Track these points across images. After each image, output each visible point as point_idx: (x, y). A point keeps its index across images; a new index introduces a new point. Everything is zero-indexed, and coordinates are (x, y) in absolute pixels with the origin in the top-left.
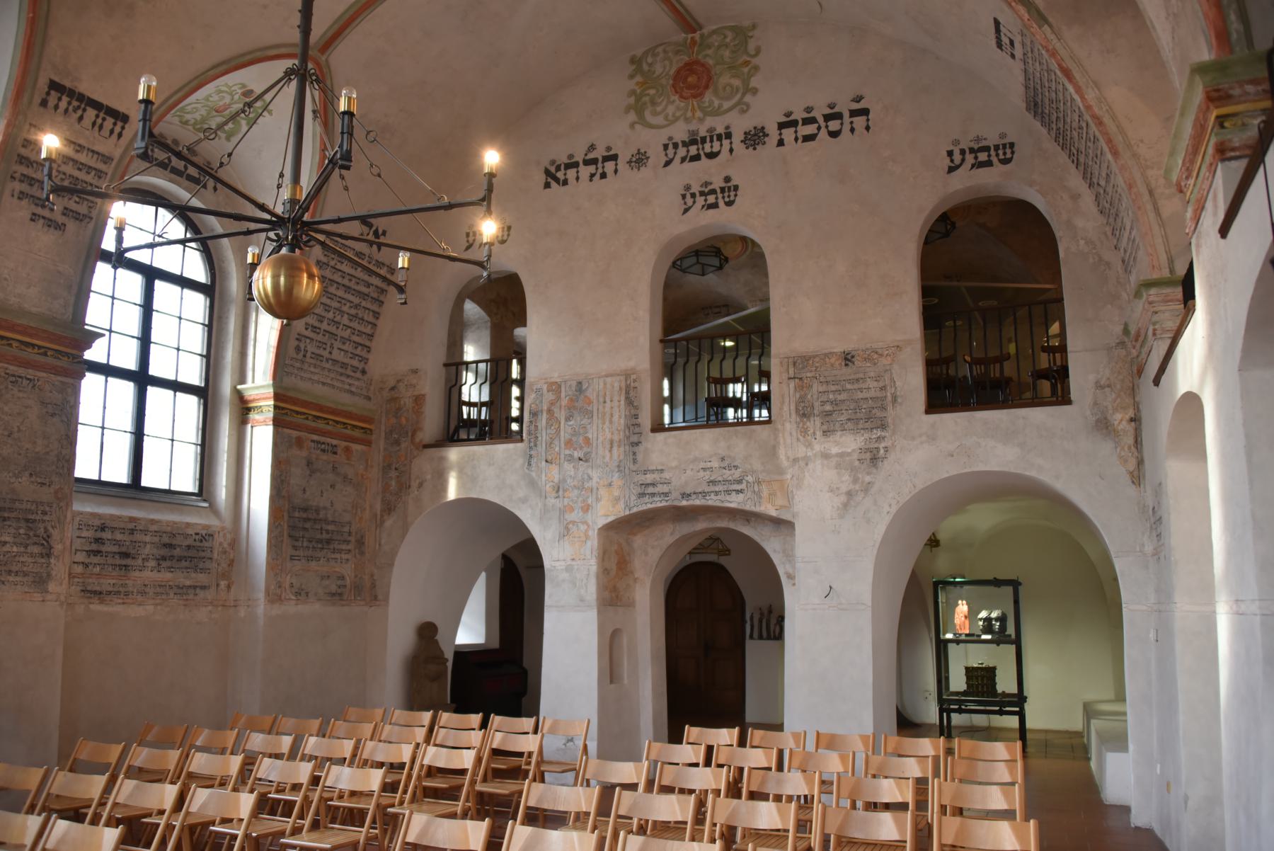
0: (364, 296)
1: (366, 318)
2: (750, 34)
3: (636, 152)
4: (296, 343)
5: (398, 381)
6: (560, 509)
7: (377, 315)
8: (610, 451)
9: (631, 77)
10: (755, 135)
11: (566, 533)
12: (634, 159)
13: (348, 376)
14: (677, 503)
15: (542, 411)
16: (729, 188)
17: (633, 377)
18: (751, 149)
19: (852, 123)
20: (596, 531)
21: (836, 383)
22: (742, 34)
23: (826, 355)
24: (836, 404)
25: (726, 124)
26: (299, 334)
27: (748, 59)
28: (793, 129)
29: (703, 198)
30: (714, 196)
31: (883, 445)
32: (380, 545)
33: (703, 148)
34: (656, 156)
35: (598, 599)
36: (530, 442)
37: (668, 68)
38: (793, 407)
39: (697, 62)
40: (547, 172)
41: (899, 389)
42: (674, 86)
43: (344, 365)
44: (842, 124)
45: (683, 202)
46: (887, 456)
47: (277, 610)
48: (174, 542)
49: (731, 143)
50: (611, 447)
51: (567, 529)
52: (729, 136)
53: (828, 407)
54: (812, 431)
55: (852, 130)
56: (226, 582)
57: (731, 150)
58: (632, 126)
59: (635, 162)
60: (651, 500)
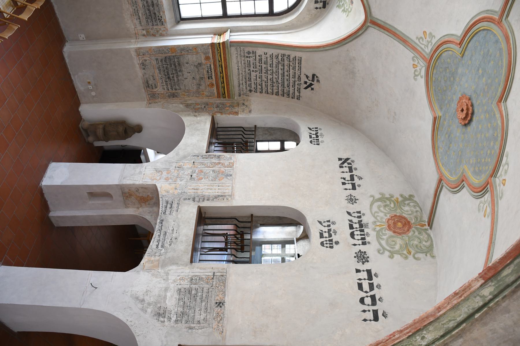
0: (283, 85)
1: (274, 88)
2: (428, 255)
3: (357, 198)
4: (251, 52)
5: (247, 106)
7: (277, 94)
8: (193, 189)
9: (401, 196)
10: (364, 257)
12: (352, 197)
13: (246, 82)
14: (159, 217)
16: (332, 244)
17: (230, 199)
18: (356, 255)
19: (369, 311)
21: (207, 297)
22: (429, 250)
23: (225, 292)
24: (194, 297)
25: (371, 242)
26: (255, 52)
27: (412, 254)
28: (366, 278)
29: (327, 231)
30: (327, 236)
31: (166, 320)
32: (172, 104)
33: (357, 231)
34: (353, 208)
35: (124, 185)
36: (205, 156)
37: (406, 213)
38: (197, 274)
39: (410, 227)
40: (348, 159)
41: (197, 331)
42: (395, 216)
43: (250, 79)
44: (368, 305)
45: (325, 221)
46: (159, 322)
47: (133, 54)
48: (155, 6)
49: (359, 245)
50: (195, 189)
51: (160, 171)
52: (364, 243)
53: (193, 292)
54: (182, 283)
55: (364, 311)
56: (146, 34)
57: (355, 245)
58: (372, 196)
59: (351, 198)
60: (164, 206)
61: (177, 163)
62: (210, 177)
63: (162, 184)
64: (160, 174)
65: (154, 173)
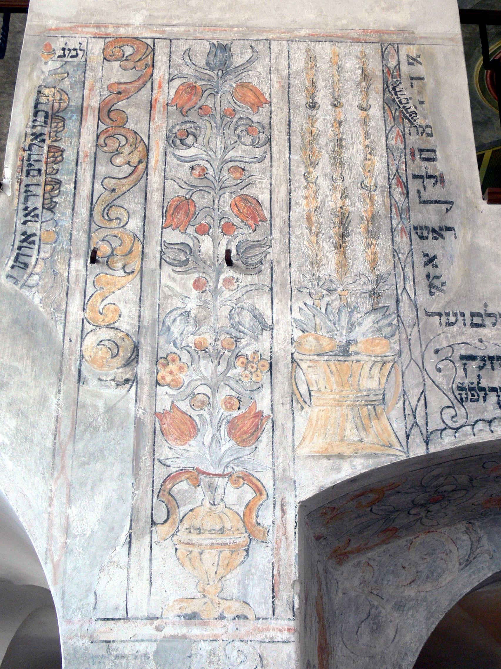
6: (138, 423)
11: (161, 514)
15: (81, 111)
17: (413, 51)
20: (292, 514)
36: (28, 194)
50: (343, 236)
61: (80, 379)
62: (231, 154)
63: (304, 451)
64: (197, 485)
65: (183, 535)
